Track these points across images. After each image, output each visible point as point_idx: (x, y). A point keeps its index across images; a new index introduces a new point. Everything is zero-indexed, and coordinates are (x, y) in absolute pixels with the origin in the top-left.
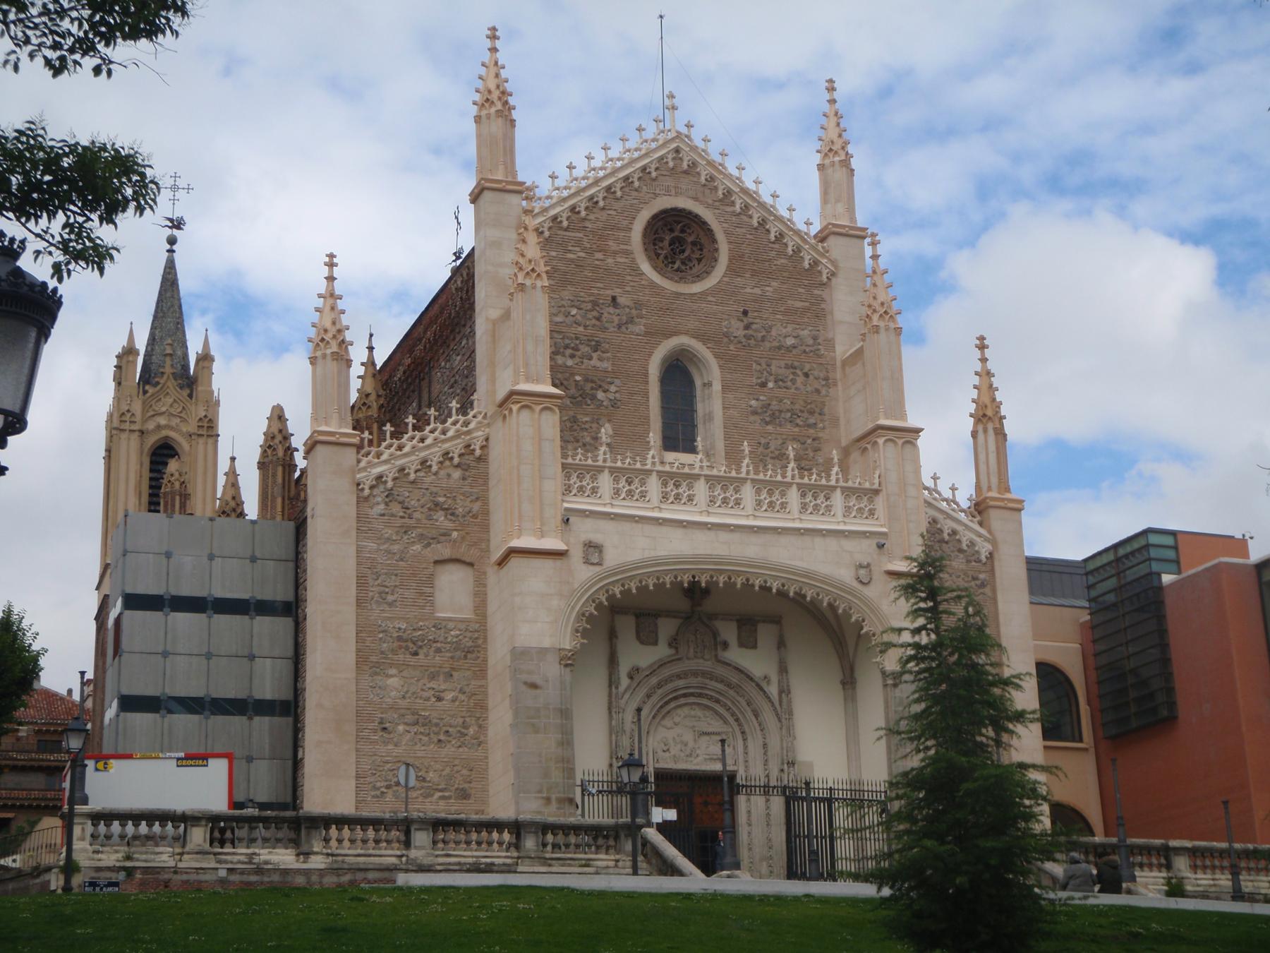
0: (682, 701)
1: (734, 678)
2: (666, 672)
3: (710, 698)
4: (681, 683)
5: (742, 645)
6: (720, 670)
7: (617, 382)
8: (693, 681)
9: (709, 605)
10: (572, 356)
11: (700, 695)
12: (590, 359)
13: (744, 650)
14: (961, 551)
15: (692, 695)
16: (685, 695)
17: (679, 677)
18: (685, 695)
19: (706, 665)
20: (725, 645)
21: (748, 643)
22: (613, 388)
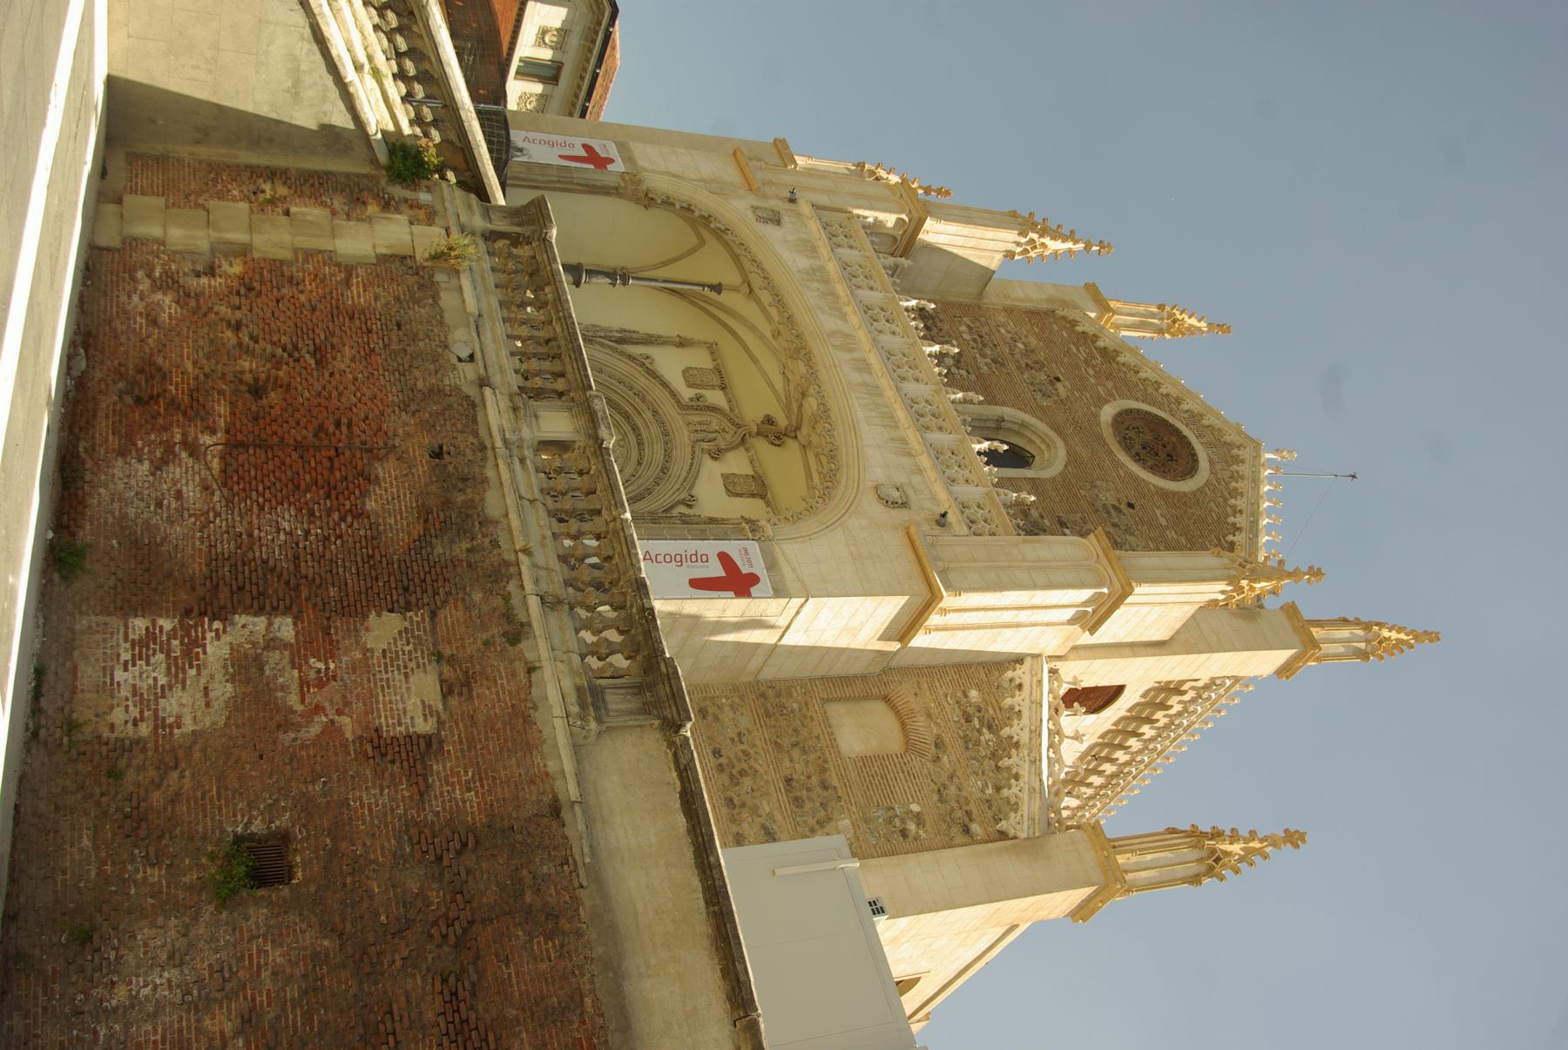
0: (627, 428)
1: (679, 467)
2: (657, 393)
3: (641, 456)
4: (648, 415)
5: (725, 477)
6: (682, 456)
7: (973, 377)
8: (654, 428)
9: (761, 446)
10: (974, 340)
11: (640, 444)
12: (984, 356)
13: (721, 481)
14: (998, 789)
15: (638, 435)
16: (635, 429)
17: (655, 413)
18: (635, 429)
19: (683, 437)
20: (716, 455)
21: (732, 486)
22: (963, 372)
